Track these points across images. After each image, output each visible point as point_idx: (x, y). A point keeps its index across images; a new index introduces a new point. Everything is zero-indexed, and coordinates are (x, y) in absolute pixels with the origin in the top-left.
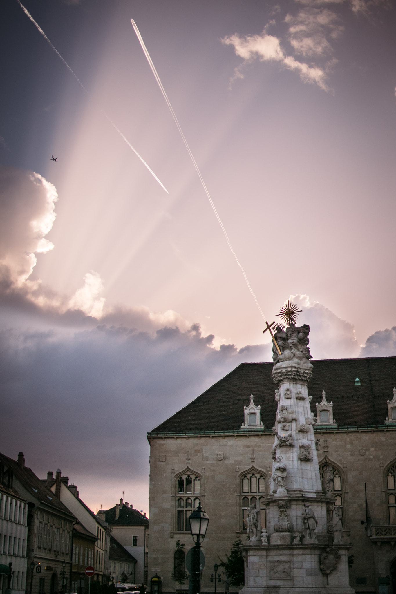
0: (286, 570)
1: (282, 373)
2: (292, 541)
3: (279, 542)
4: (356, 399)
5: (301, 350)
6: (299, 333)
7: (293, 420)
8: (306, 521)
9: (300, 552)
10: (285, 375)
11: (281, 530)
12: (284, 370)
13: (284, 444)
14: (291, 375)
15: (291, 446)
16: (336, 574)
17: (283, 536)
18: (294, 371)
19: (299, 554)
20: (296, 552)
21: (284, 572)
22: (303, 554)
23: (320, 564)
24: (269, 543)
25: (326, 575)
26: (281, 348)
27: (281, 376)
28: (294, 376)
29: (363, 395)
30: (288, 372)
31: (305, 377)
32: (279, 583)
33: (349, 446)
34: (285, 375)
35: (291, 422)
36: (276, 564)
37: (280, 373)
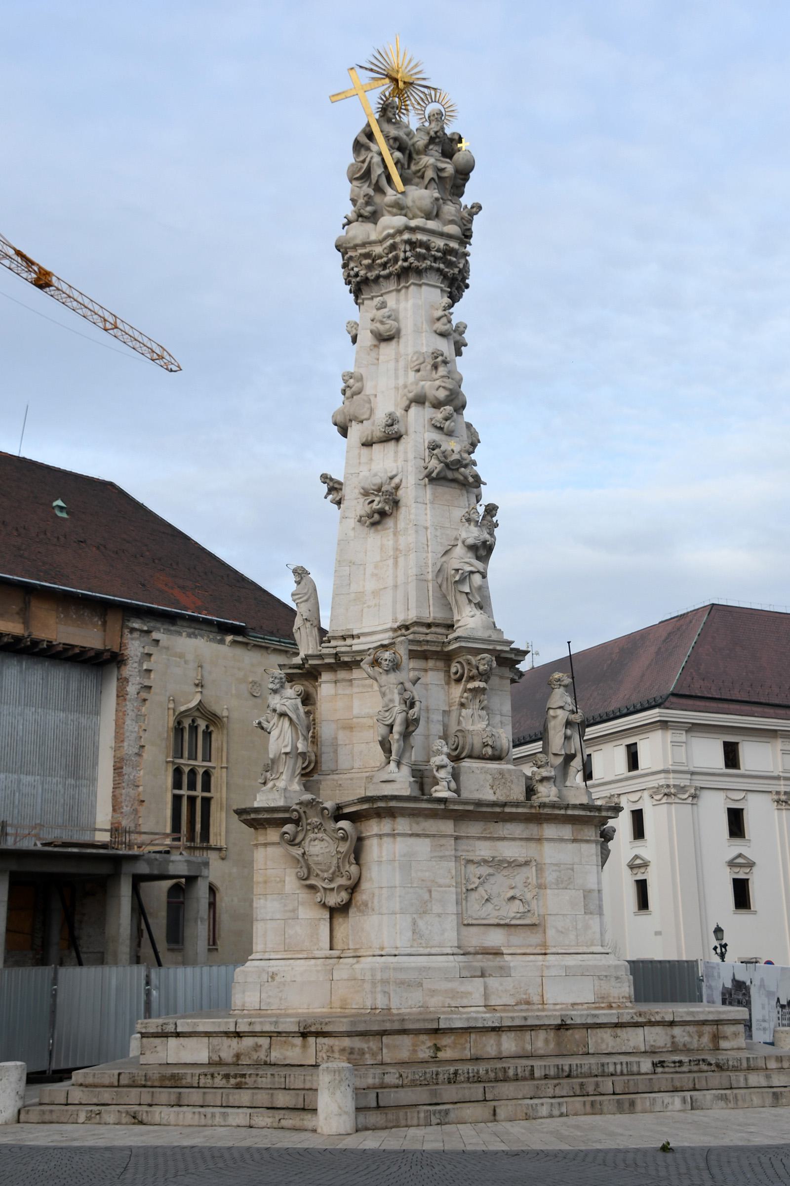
0: (517, 892)
1: (428, 248)
3: (488, 795)
9: (566, 831)
10: (436, 259)
11: (489, 751)
12: (440, 243)
17: (501, 773)
19: (562, 840)
20: (550, 831)
21: (513, 898)
22: (575, 841)
24: (457, 791)
27: (420, 257)
32: (495, 938)
34: (436, 259)
36: (484, 870)
37: (422, 244)
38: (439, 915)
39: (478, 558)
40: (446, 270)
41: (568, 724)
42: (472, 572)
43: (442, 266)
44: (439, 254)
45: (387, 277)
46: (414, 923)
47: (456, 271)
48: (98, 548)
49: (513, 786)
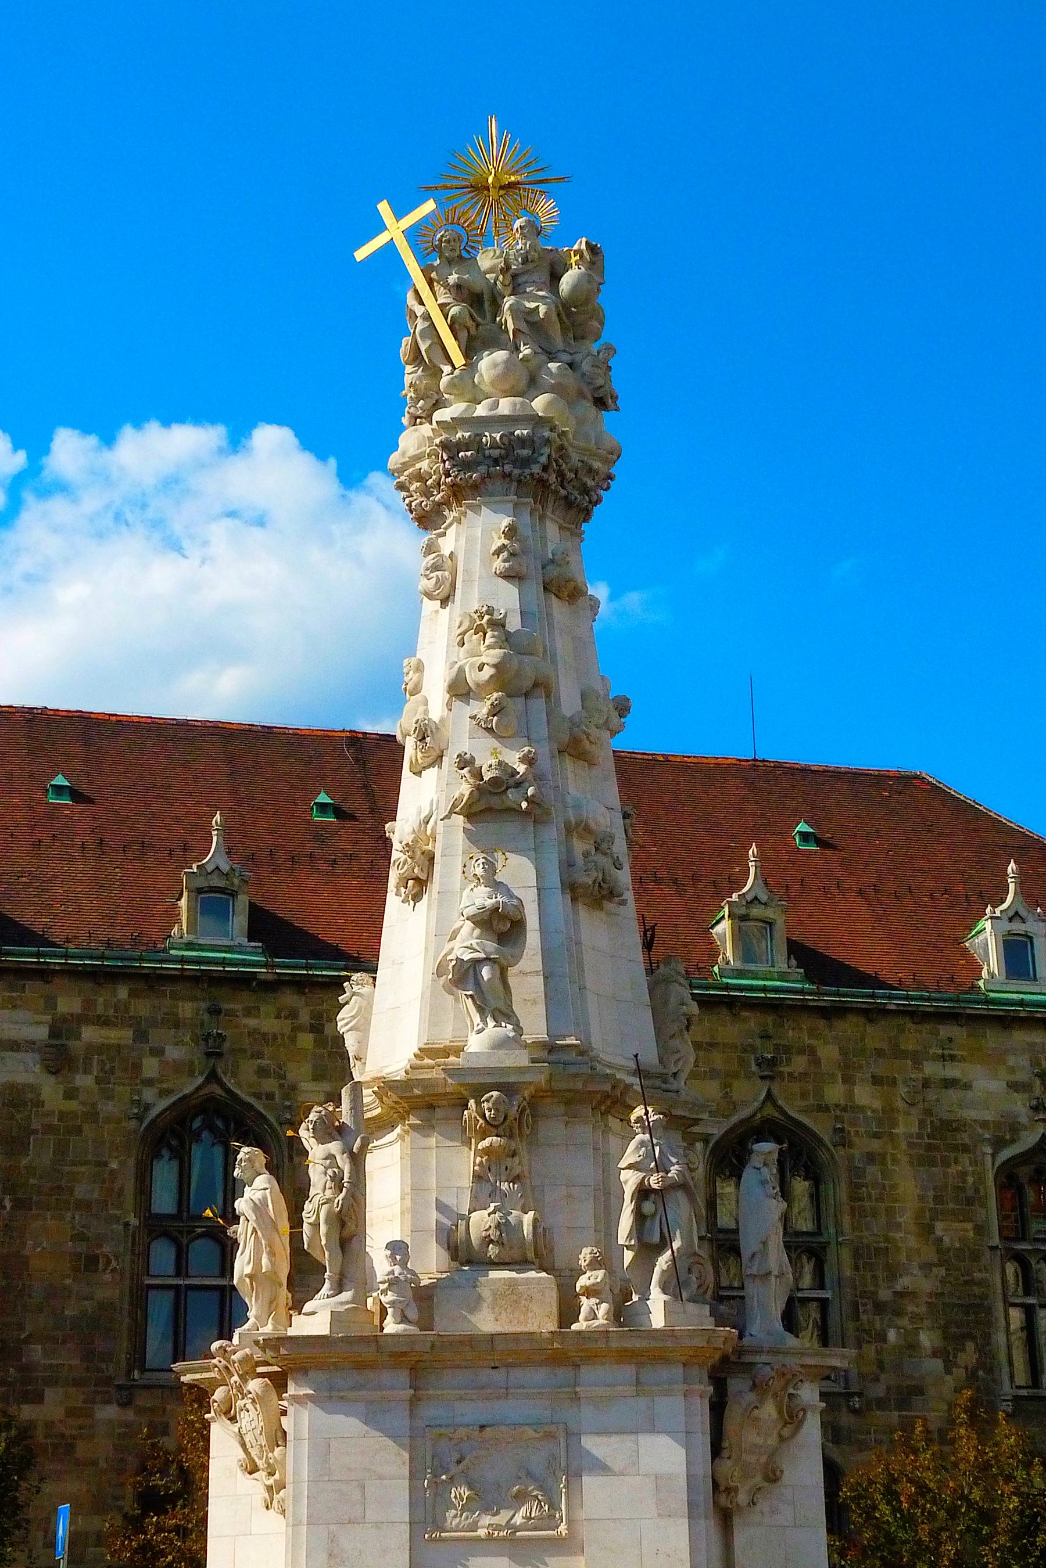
2: (568, 1312)
4: (324, 867)
5: (566, 357)
6: (555, 278)
7: (536, 685)
8: (648, 1207)
10: (496, 462)
13: (495, 802)
14: (525, 463)
15: (537, 814)
16: (774, 1511)
18: (548, 441)
23: (716, 1451)
25: (725, 1518)
26: (463, 335)
28: (545, 468)
29: (351, 857)
30: (510, 444)
31: (585, 491)
33: (306, 1040)
34: (496, 462)
35: (527, 695)
38: (378, 1525)
39: (502, 938)
40: (517, 472)
41: (643, 1193)
42: (476, 963)
43: (508, 468)
44: (496, 453)
45: (446, 503)
46: (333, 1539)
47: (536, 469)
48: (861, 893)
49: (534, 1306)
